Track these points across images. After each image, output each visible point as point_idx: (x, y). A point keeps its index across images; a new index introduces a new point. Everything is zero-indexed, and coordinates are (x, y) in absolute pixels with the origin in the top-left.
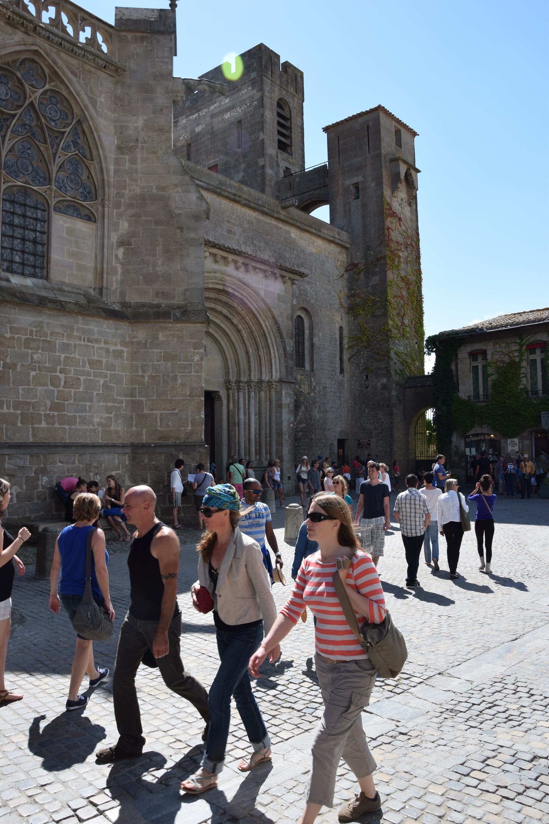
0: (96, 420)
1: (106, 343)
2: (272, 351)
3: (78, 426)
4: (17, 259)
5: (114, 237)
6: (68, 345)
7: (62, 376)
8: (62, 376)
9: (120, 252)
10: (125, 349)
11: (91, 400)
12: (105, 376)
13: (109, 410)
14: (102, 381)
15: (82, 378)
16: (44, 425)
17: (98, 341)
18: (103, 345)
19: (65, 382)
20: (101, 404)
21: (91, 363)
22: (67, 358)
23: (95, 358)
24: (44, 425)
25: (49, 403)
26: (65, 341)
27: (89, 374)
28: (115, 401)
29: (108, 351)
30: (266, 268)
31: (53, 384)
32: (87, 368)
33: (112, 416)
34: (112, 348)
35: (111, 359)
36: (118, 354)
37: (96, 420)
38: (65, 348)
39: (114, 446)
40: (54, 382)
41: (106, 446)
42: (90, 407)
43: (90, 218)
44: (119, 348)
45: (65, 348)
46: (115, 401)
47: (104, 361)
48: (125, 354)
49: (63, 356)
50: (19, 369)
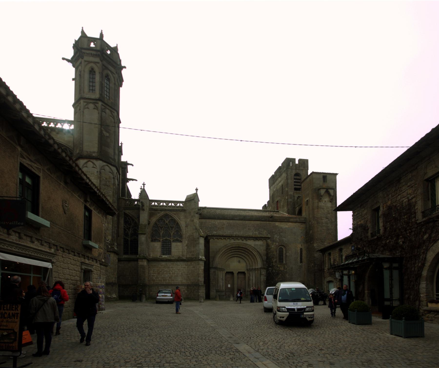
0: (179, 280)
1: (181, 266)
2: (258, 260)
3: (175, 281)
4: (165, 252)
5: (185, 245)
6: (172, 267)
7: (171, 272)
8: (171, 272)
9: (186, 248)
10: (186, 266)
11: (178, 276)
12: (181, 272)
13: (182, 278)
14: (180, 273)
15: (176, 273)
16: (167, 281)
17: (180, 266)
18: (181, 266)
19: (172, 273)
20: (181, 277)
21: (178, 270)
22: (172, 270)
23: (179, 269)
24: (167, 281)
25: (169, 278)
26: (172, 266)
27: (177, 272)
28: (184, 276)
29: (182, 267)
30: (254, 238)
31: (169, 274)
32: (177, 271)
33: (183, 279)
34: (183, 266)
35: (183, 269)
36: (185, 267)
37: (179, 280)
38: (172, 267)
39: (183, 285)
40: (170, 274)
41: (181, 285)
42: (178, 278)
43: (181, 242)
44: (185, 266)
45: (172, 267)
46: (184, 276)
47: (181, 269)
48: (186, 267)
49: (171, 269)
50: (162, 272)
